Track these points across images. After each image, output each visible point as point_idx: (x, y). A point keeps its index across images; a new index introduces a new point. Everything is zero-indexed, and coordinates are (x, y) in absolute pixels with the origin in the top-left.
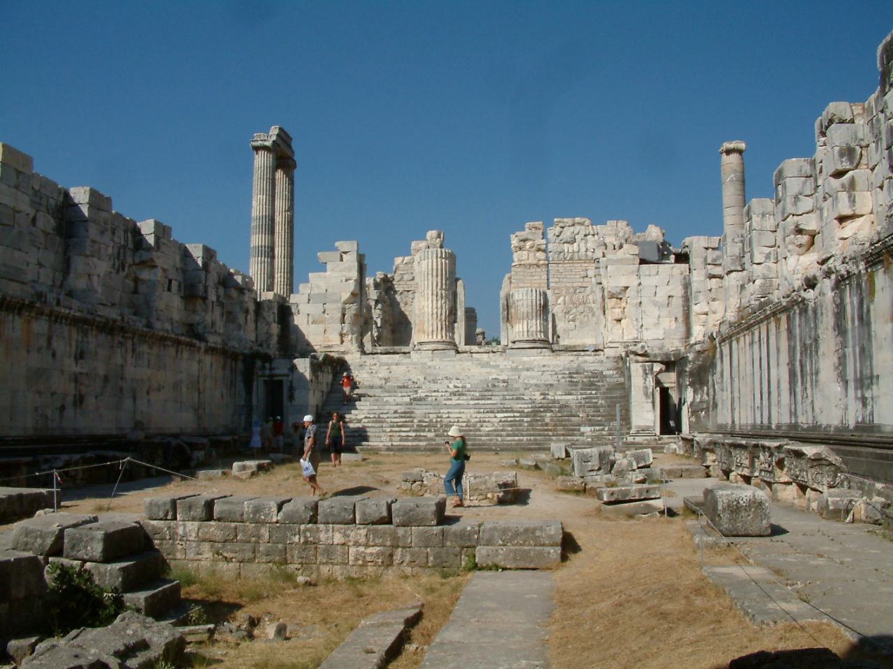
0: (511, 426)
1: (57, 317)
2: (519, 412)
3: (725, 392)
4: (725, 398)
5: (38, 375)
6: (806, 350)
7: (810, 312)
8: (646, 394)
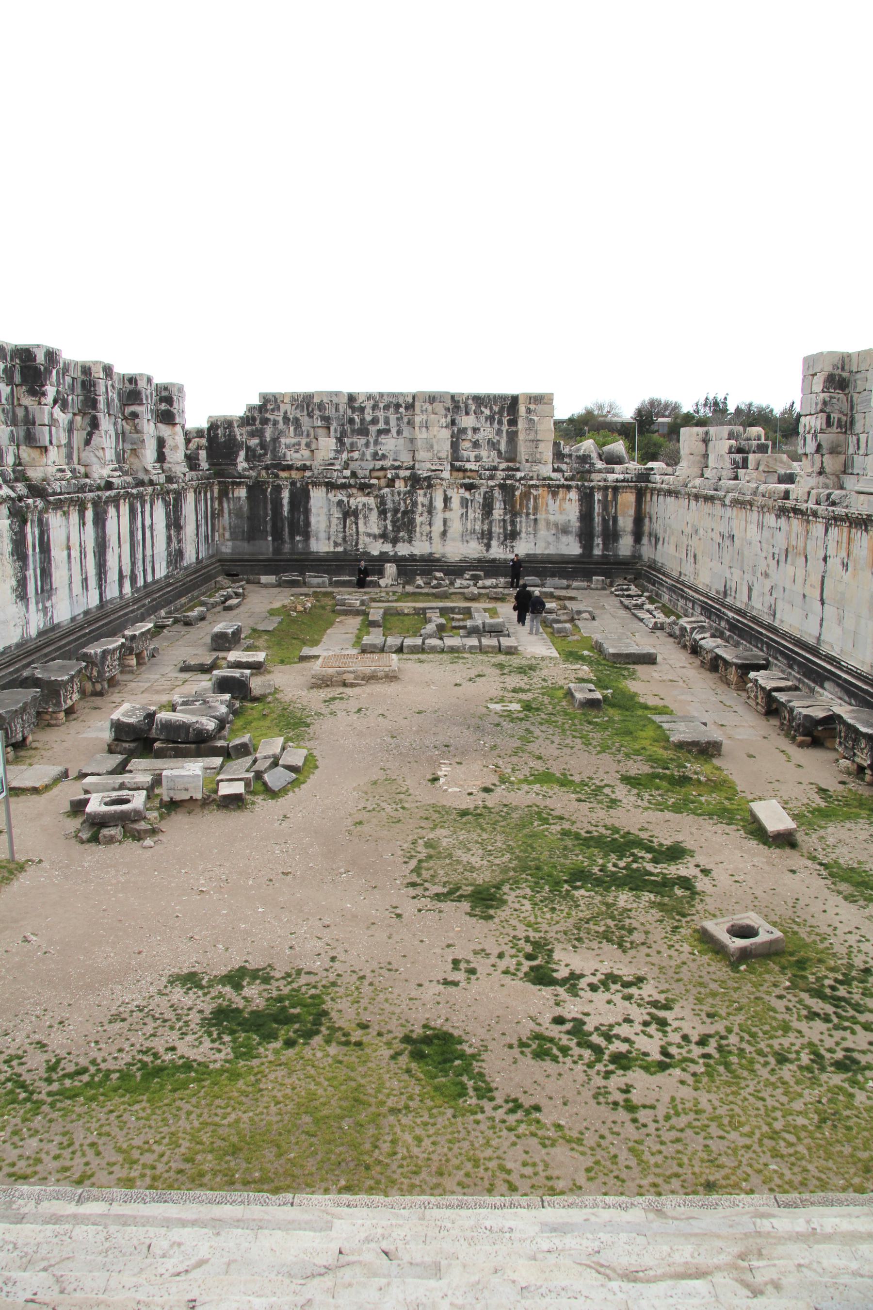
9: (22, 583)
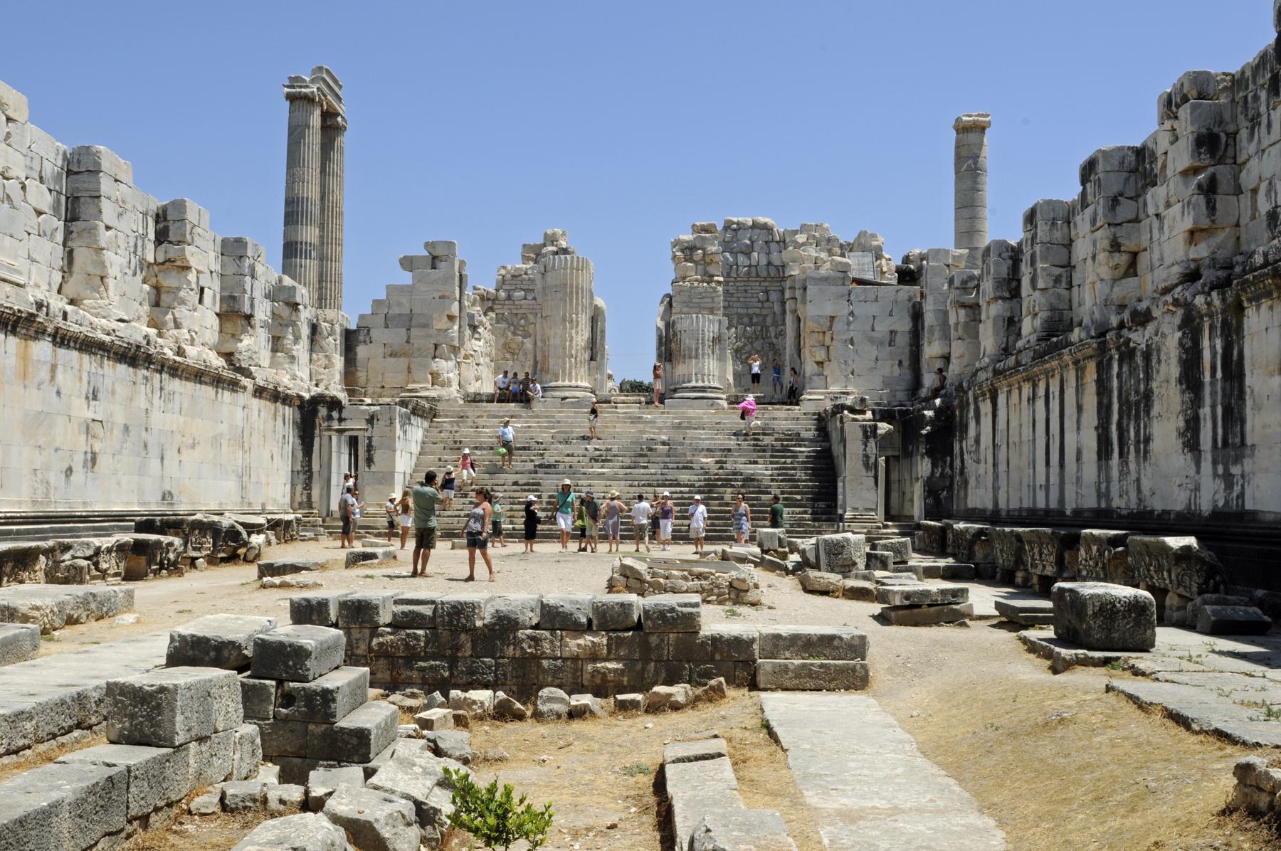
0: (676, 505)
1: (63, 339)
2: (687, 486)
3: (982, 464)
4: (981, 471)
5: (37, 422)
6: (1130, 409)
7: (1139, 360)
8: (866, 466)
9: (1192, 425)
